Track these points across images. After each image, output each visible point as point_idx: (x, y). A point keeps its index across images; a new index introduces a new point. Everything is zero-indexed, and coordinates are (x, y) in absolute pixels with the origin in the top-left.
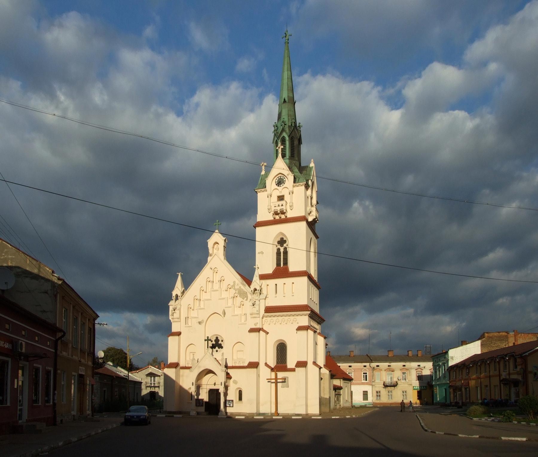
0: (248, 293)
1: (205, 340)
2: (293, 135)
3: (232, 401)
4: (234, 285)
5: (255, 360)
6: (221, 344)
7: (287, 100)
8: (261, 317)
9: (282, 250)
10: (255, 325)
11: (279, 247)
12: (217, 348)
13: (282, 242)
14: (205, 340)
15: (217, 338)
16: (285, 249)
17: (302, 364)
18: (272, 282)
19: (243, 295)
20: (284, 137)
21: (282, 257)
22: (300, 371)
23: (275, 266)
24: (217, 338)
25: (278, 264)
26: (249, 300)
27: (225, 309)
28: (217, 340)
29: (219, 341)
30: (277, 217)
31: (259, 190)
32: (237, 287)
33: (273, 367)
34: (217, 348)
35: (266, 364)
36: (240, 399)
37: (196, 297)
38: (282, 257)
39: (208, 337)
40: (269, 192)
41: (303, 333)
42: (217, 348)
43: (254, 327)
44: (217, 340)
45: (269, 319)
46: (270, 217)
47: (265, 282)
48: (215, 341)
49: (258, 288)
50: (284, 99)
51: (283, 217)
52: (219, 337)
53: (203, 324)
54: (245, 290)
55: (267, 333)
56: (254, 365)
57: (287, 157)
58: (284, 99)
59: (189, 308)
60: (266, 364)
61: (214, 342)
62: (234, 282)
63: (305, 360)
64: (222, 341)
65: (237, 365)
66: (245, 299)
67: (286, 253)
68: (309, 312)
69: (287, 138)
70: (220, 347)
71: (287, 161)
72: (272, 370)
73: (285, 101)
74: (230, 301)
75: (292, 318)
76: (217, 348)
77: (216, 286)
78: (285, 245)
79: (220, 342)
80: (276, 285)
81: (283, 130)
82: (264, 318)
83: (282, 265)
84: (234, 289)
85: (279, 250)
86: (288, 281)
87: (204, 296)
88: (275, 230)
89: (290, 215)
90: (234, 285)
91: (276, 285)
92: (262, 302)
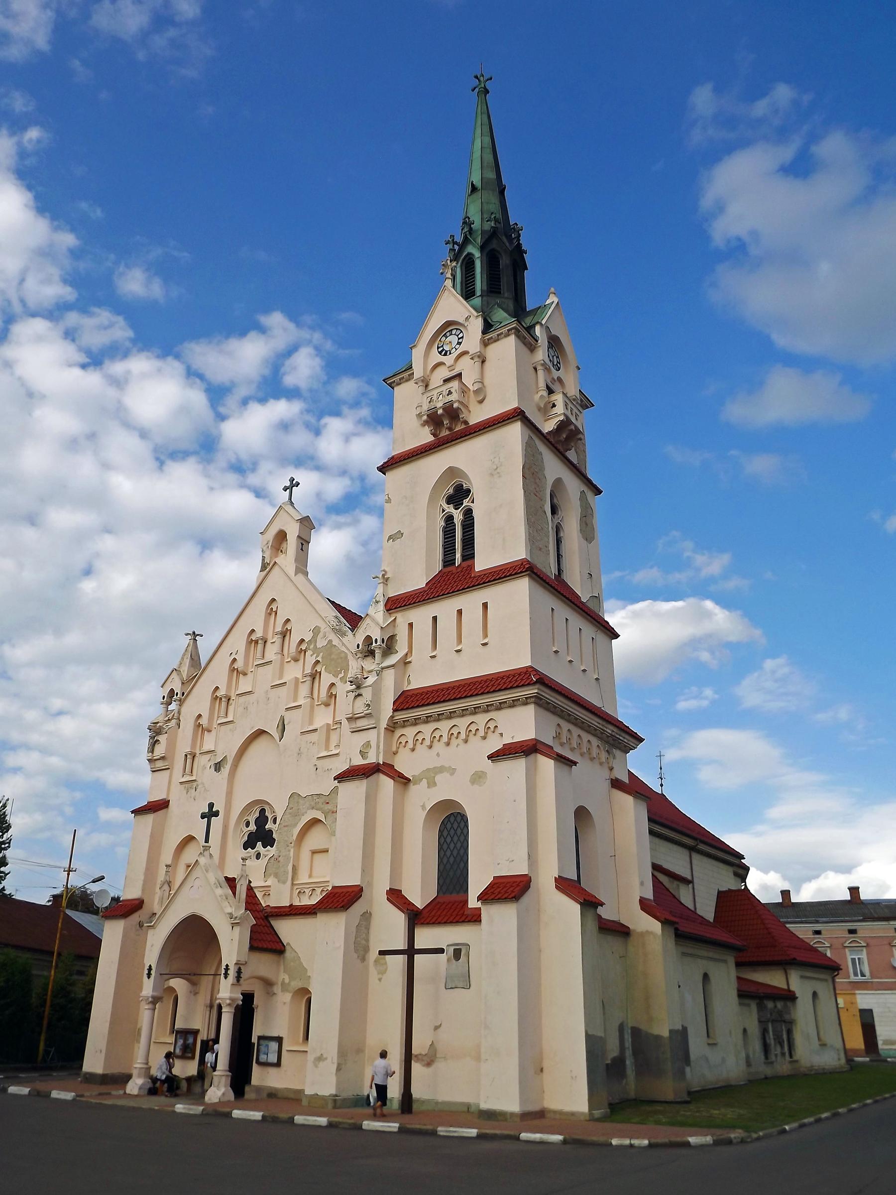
0: (350, 657)
1: (203, 817)
2: (494, 245)
3: (279, 1040)
4: (314, 640)
5: (351, 878)
6: (271, 832)
7: (478, 184)
8: (384, 724)
9: (458, 516)
10: (363, 754)
11: (450, 509)
12: (259, 844)
14: (203, 817)
15: (263, 811)
16: (468, 513)
17: (509, 890)
18: (421, 616)
19: (338, 664)
20: (470, 257)
21: (459, 537)
22: (501, 918)
23: (438, 567)
24: (263, 811)
25: (448, 561)
27: (288, 716)
28: (262, 820)
29: (266, 819)
31: (397, 379)
32: (321, 643)
33: (419, 903)
34: (259, 844)
35: (396, 897)
37: (218, 694)
38: (459, 537)
39: (211, 805)
40: (418, 371)
41: (518, 766)
43: (358, 761)
44: (262, 820)
46: (426, 436)
47: (403, 618)
48: (257, 821)
49: (376, 634)
50: (472, 184)
51: (459, 427)
52: (267, 808)
53: (226, 770)
54: (343, 649)
55: (403, 781)
56: (341, 899)
57: (478, 293)
58: (473, 185)
59: (200, 729)
60: (396, 897)
61: (253, 827)
62: (316, 631)
63: (523, 870)
64: (275, 821)
66: (342, 675)
68: (532, 691)
69: (477, 254)
71: (477, 301)
72: (417, 918)
73: (474, 189)
74: (304, 690)
75: (481, 719)
77: (272, 652)
80: (435, 619)
81: (466, 241)
82: (399, 732)
84: (316, 650)
85: (449, 519)
86: (470, 602)
87: (245, 685)
88: (434, 466)
89: (477, 415)
90: (314, 640)
91: (435, 619)
92: (389, 677)
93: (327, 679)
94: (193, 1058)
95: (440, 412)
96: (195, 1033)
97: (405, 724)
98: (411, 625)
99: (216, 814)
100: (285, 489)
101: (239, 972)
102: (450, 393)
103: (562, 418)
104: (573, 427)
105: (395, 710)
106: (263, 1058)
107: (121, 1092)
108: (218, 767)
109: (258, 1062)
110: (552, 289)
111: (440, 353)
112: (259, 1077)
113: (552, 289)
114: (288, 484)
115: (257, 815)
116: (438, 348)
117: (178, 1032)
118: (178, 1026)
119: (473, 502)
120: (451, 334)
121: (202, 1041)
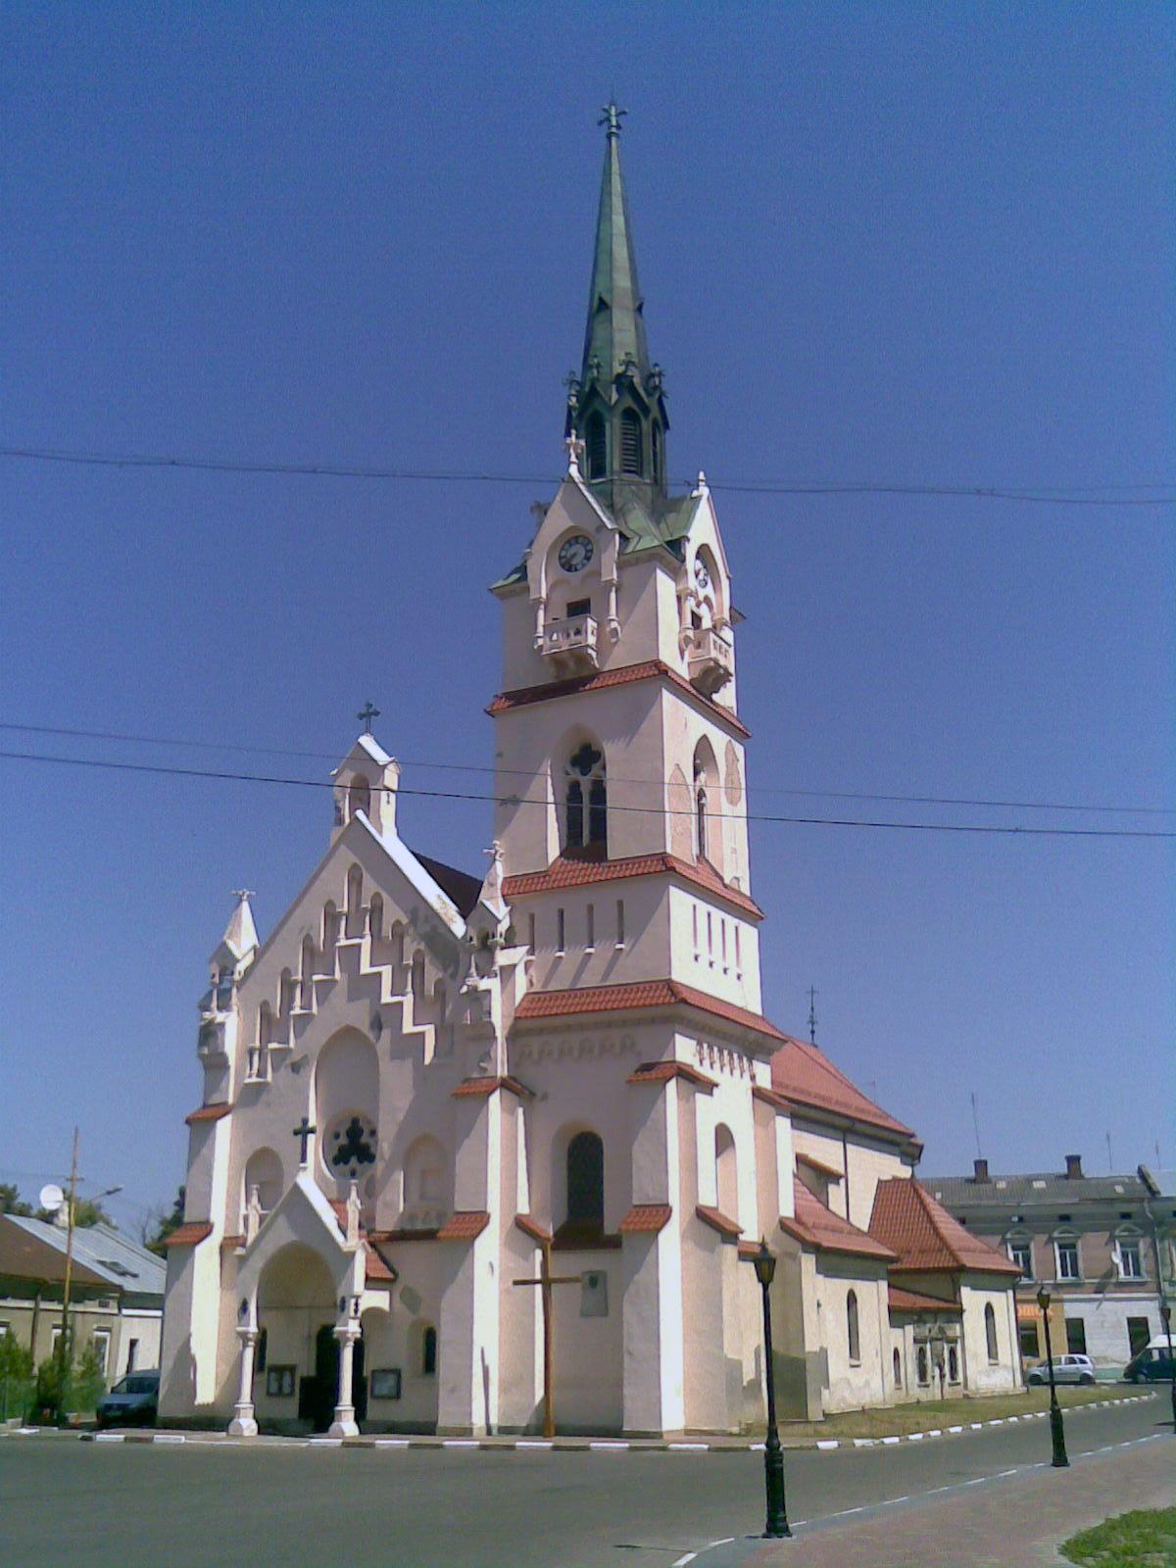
1: (296, 1133)
3: (397, 1373)
9: (586, 788)
13: (587, 757)
15: (355, 1122)
24: (355, 1122)
26: (462, 971)
28: (355, 1131)
30: (568, 676)
36: (430, 1365)
39: (305, 1121)
42: (353, 1161)
44: (355, 1131)
45: (535, 1043)
46: (547, 677)
48: (349, 1134)
50: (601, 299)
58: (601, 299)
61: (343, 1140)
64: (373, 1133)
65: (419, 1226)
67: (599, 793)
70: (366, 1155)
76: (353, 1161)
78: (596, 768)
79: (365, 1139)
83: (586, 840)
85: (575, 788)
93: (432, 974)
94: (292, 1394)
95: (566, 656)
96: (292, 1369)
97: (529, 1032)
98: (532, 917)
99: (312, 1131)
100: (361, 716)
101: (356, 1305)
102: (578, 632)
103: (712, 664)
104: (722, 671)
105: (517, 1019)
106: (377, 1392)
107: (224, 1434)
108: (296, 1068)
109: (374, 1397)
110: (702, 476)
111: (563, 566)
112: (374, 1411)
113: (702, 476)
114: (364, 710)
115: (348, 1125)
116: (560, 558)
117: (275, 1369)
118: (269, 1360)
119: (604, 768)
120: (577, 543)
121: (303, 1380)
